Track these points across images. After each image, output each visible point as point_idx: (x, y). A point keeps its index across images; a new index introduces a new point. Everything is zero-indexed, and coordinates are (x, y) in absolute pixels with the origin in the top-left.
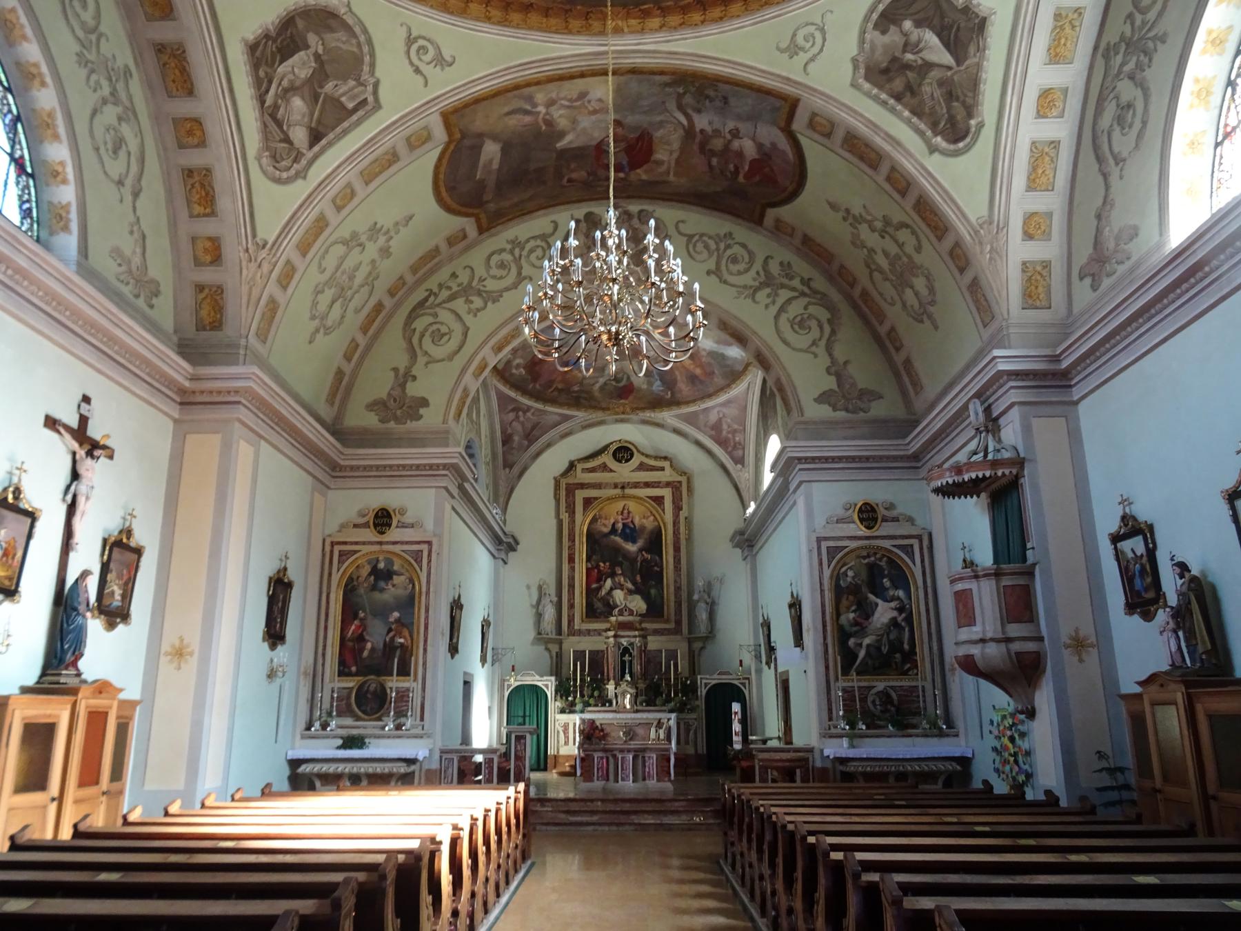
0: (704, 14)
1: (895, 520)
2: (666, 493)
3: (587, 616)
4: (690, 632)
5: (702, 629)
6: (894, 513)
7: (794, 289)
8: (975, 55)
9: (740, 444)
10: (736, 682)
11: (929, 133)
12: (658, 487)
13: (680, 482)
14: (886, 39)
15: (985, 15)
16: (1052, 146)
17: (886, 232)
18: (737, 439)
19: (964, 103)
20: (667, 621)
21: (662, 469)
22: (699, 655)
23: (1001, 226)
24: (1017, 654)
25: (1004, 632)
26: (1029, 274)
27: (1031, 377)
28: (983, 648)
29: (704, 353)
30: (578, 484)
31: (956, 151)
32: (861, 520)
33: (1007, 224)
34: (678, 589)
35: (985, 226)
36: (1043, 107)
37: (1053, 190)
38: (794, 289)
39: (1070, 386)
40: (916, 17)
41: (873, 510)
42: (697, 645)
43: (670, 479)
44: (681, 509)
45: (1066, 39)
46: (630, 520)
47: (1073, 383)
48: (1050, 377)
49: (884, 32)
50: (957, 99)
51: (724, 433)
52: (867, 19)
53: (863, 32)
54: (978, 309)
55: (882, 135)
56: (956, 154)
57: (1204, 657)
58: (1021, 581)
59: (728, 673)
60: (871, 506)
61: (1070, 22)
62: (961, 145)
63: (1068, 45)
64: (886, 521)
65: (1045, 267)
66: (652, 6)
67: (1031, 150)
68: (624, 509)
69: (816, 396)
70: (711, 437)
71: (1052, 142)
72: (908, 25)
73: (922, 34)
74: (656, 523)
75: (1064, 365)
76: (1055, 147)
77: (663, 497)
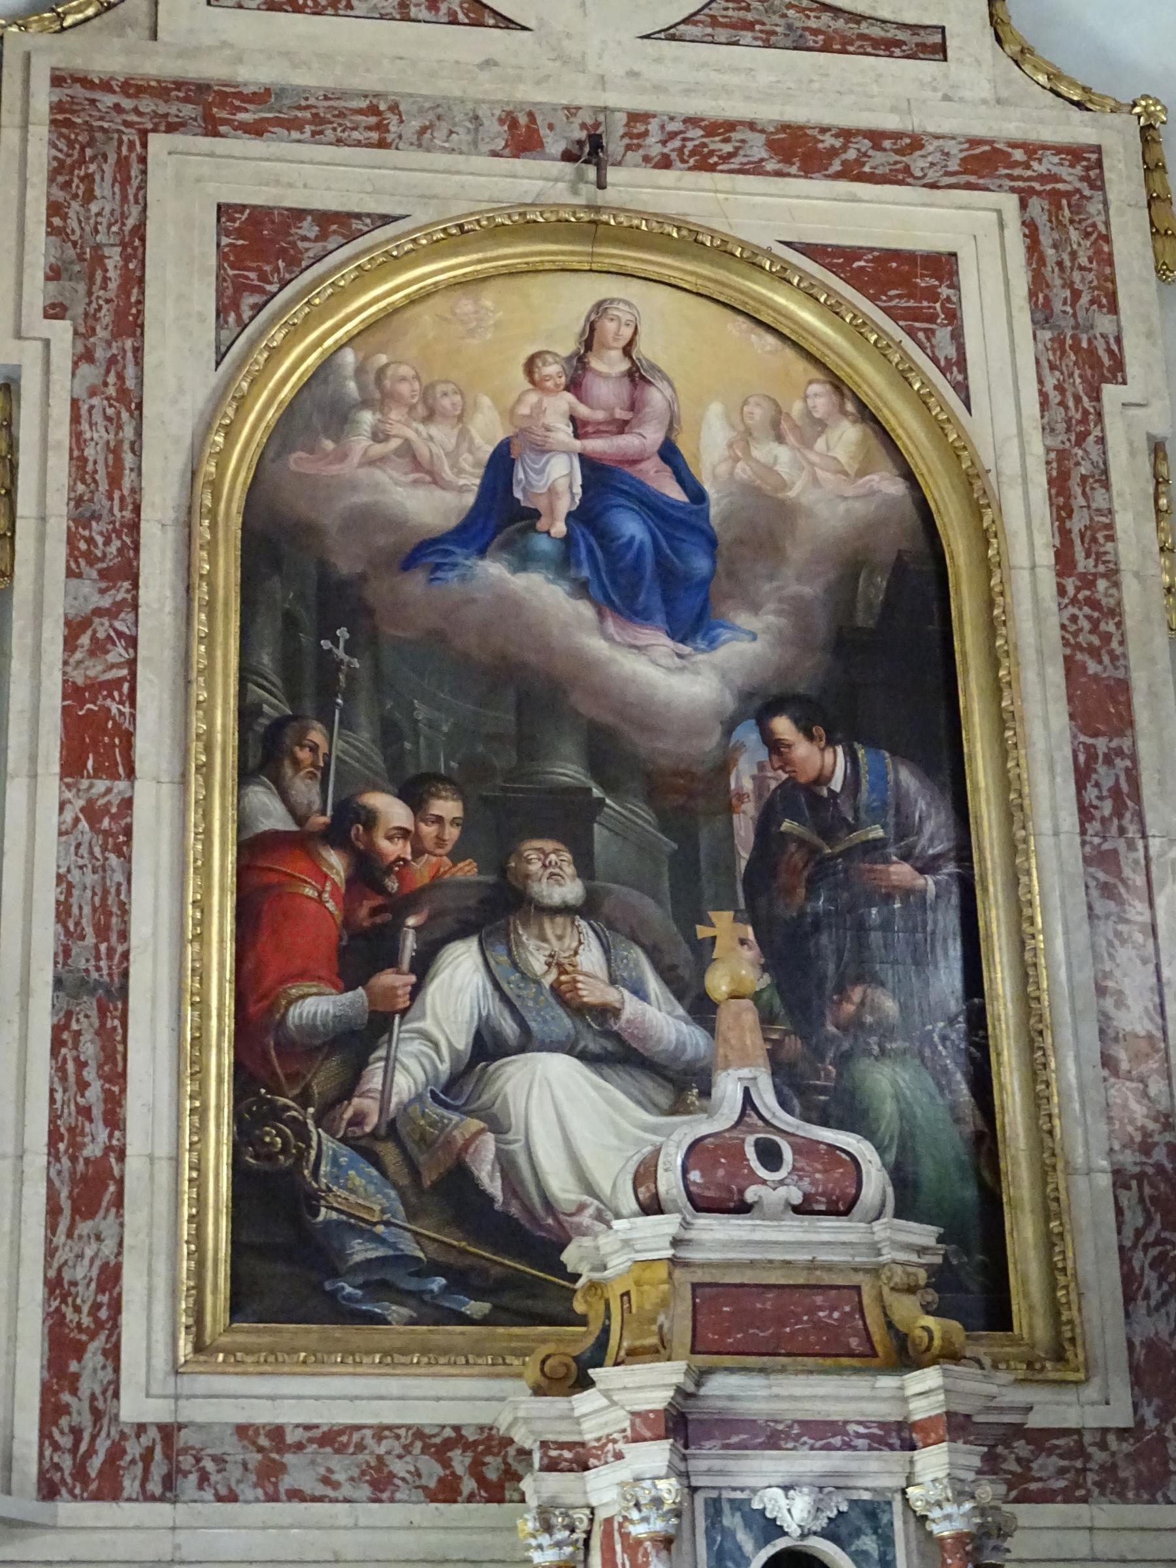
3: (238, 1308)
12: (899, 177)
30: (164, 90)
44: (1117, 371)
46: (651, 436)
68: (590, 340)
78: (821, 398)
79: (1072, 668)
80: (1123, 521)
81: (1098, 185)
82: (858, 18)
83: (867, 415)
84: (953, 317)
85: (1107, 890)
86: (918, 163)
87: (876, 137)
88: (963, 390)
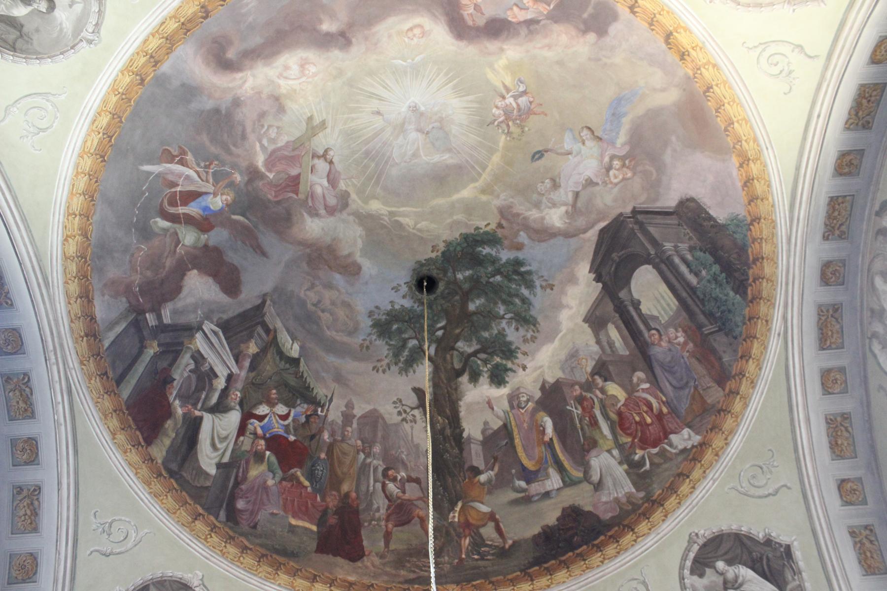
0: (532, 584)
8: (794, 579)
14: (705, 581)
15: (788, 543)
40: (726, 557)
45: (870, 552)
49: (701, 575)
52: (682, 568)
53: (682, 578)
61: (866, 537)
63: (875, 556)
66: (483, 581)
72: (720, 565)
73: (736, 571)
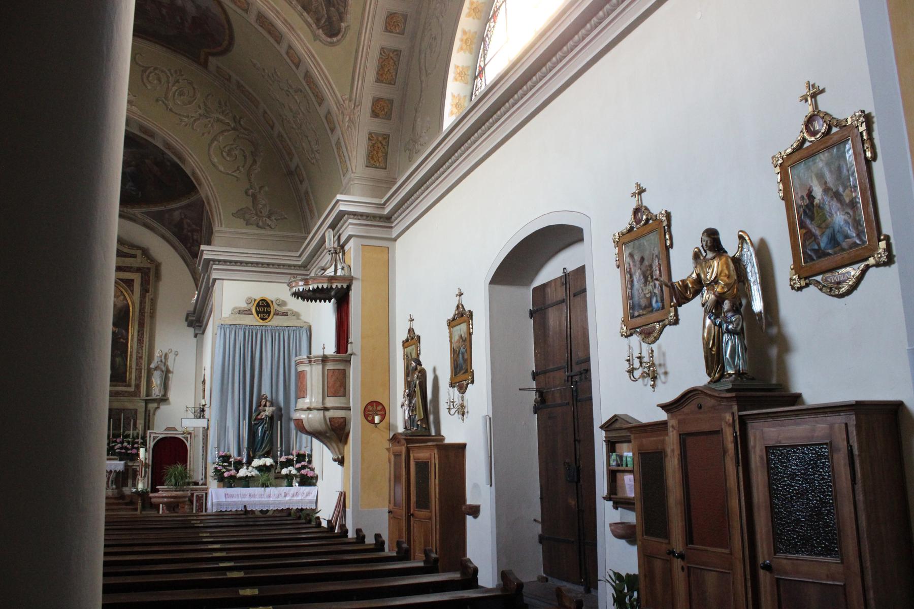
1: (285, 314)
2: (136, 277)
4: (148, 395)
5: (156, 392)
6: (284, 309)
7: (228, 124)
9: (197, 241)
10: (180, 436)
11: (314, 26)
12: (130, 271)
13: (149, 269)
16: (395, 53)
17: (289, 92)
18: (195, 237)
19: (338, 10)
20: (129, 386)
21: (134, 256)
22: (154, 414)
23: (357, 104)
24: (331, 419)
25: (323, 403)
26: (373, 142)
27: (365, 217)
28: (309, 414)
29: (168, 164)
31: (331, 43)
32: (258, 313)
33: (360, 103)
34: (139, 358)
35: (347, 102)
36: (389, 24)
37: (394, 84)
38: (228, 124)
39: (391, 227)
41: (268, 305)
42: (152, 406)
43: (142, 265)
47: (393, 225)
48: (378, 219)
50: (334, 6)
51: (185, 231)
54: (341, 162)
55: (282, 20)
56: (332, 44)
57: (419, 423)
58: (341, 366)
59: (175, 429)
60: (267, 303)
62: (335, 39)
64: (277, 315)
65: (384, 139)
67: (381, 53)
69: (235, 212)
70: (174, 234)
71: (397, 51)
74: (125, 302)
75: (386, 211)
76: (397, 55)
77: (133, 281)
78: (119, 293)
79: (139, 322)
80: (146, 307)
81: (150, 272)
82: (128, 254)
83: (124, 295)
84: (133, 286)
85: (139, 343)
86: (132, 270)
87: (127, 267)
88: (133, 294)
